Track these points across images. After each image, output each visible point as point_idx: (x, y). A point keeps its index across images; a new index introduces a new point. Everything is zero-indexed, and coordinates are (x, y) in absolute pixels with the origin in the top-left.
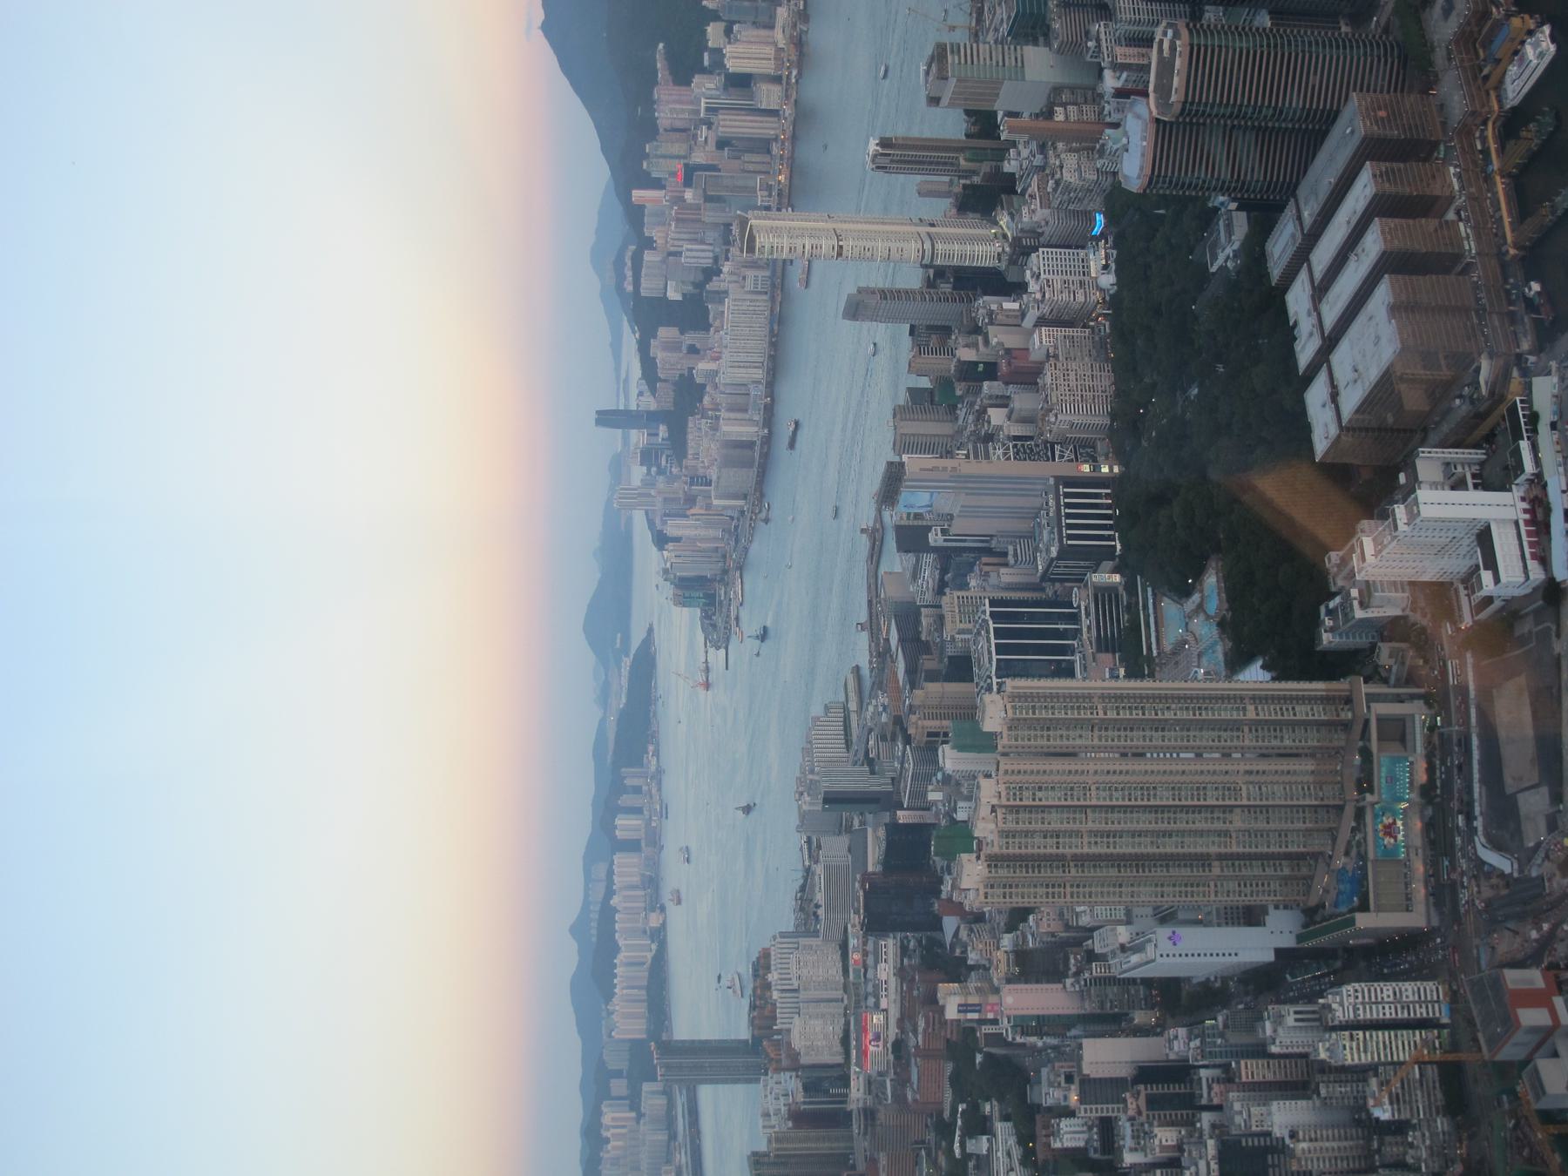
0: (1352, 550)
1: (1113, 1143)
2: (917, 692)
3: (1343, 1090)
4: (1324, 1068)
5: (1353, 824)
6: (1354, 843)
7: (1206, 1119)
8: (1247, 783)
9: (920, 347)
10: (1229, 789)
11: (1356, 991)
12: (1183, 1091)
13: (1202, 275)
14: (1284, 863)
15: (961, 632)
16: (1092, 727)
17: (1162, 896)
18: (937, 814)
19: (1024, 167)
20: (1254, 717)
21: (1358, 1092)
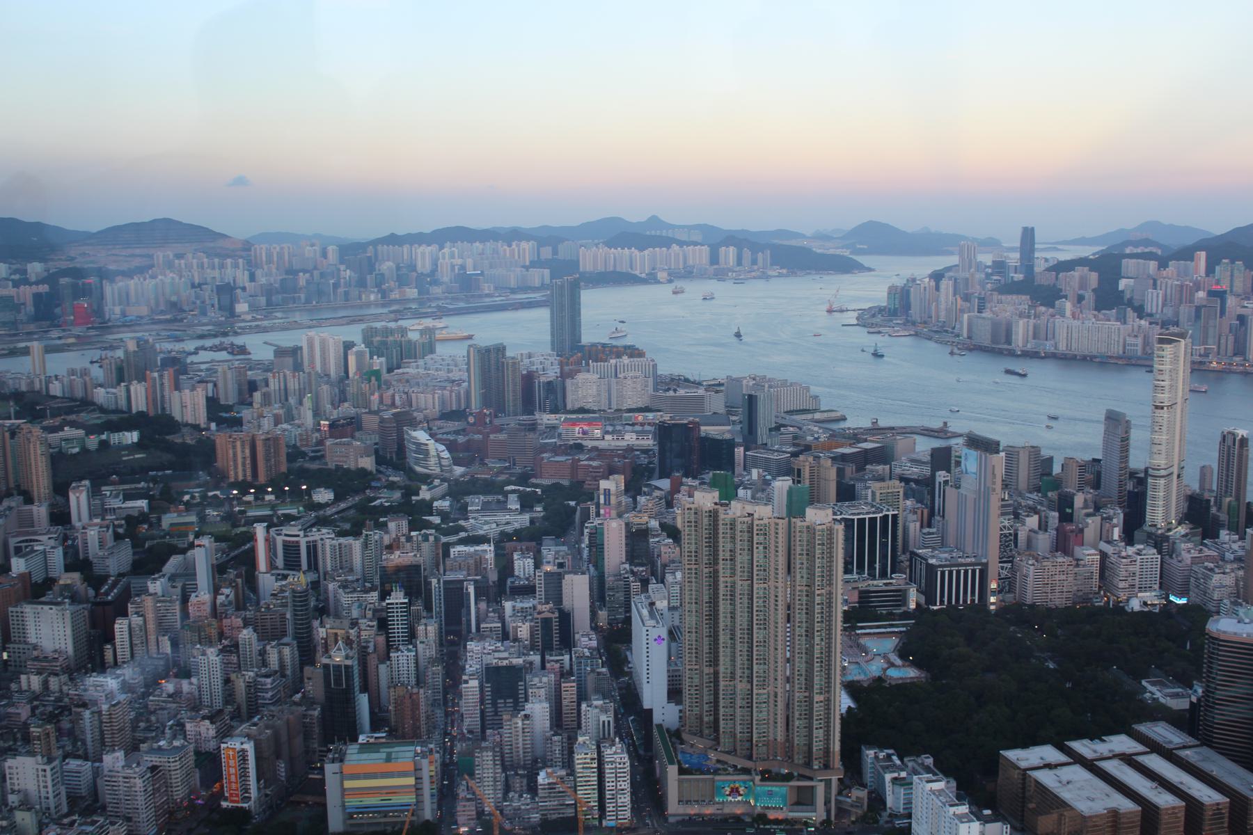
0: (935, 774)
1: (519, 595)
2: (830, 461)
3: (557, 752)
4: (572, 740)
5: (739, 767)
6: (726, 766)
7: (536, 658)
8: (768, 693)
9: (1083, 467)
10: (764, 681)
11: (624, 764)
12: (555, 643)
13: (1139, 675)
14: (712, 718)
15: (873, 493)
16: (809, 586)
18: (741, 475)
19: (1224, 546)
20: (815, 700)
21: (556, 762)
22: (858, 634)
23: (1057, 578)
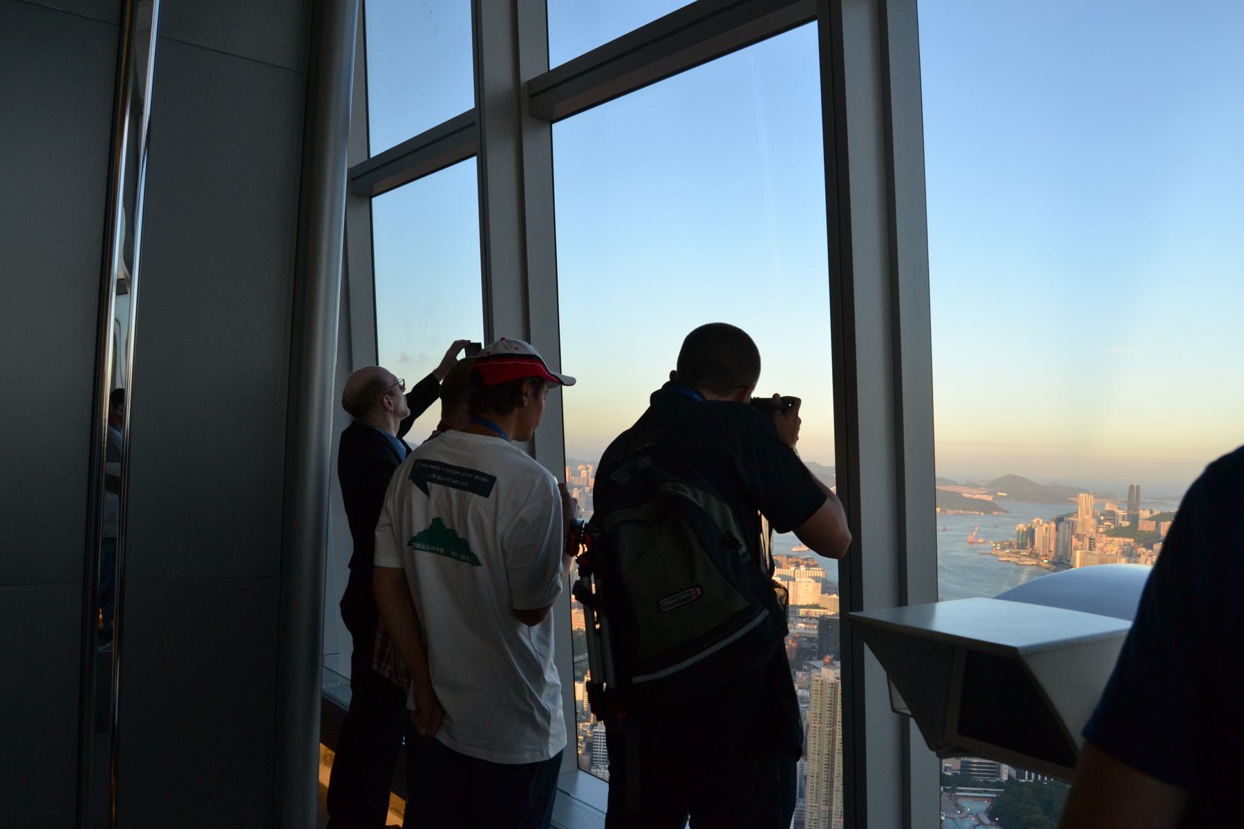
17: (812, 776)
22: (957, 796)
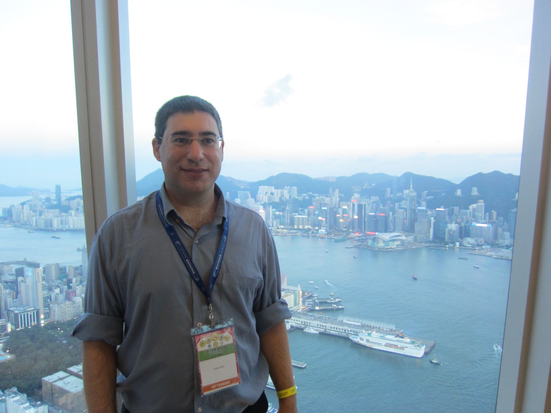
0: (16, 394)
9: (76, 268)
23: (67, 309)
